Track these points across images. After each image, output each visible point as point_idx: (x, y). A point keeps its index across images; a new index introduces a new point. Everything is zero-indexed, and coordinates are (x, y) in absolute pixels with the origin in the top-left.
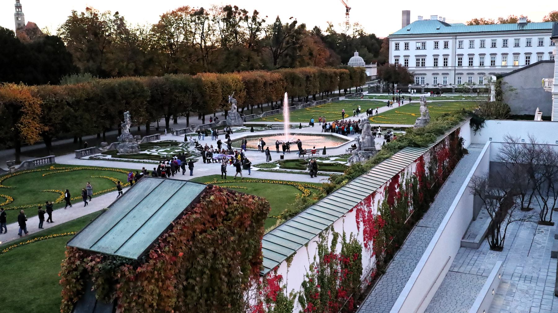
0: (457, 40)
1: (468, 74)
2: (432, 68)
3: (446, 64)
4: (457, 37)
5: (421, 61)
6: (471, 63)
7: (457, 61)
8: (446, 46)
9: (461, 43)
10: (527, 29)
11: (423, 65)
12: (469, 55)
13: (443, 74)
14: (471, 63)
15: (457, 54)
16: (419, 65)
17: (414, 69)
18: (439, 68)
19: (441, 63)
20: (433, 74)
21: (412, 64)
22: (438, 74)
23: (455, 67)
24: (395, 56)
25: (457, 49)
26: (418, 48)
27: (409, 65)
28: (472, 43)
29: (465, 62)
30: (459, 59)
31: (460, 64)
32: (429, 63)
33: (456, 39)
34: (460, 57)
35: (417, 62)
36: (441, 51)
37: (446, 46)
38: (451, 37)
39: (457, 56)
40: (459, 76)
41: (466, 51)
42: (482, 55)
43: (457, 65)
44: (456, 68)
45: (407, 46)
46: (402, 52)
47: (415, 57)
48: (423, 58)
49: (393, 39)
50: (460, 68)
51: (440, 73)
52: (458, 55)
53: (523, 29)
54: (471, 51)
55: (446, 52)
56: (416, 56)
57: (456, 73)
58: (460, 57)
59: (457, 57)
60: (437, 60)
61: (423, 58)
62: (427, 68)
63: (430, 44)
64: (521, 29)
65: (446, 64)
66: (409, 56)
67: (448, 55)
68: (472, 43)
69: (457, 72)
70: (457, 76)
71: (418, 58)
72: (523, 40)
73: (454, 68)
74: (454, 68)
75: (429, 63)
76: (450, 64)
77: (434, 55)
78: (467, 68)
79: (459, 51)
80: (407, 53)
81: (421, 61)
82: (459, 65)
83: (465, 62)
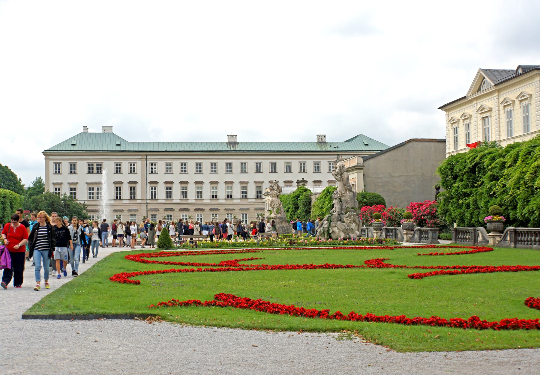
3: (133, 195)
4: (148, 157)
5: (95, 191)
6: (169, 195)
7: (149, 191)
8: (133, 169)
10: (239, 149)
12: (166, 183)
13: (130, 210)
14: (169, 195)
15: (148, 181)
16: (93, 198)
18: (124, 202)
19: (126, 193)
21: (82, 196)
22: (122, 210)
23: (147, 200)
24: (54, 184)
25: (148, 175)
27: (78, 197)
28: (169, 166)
29: (161, 193)
30: (152, 189)
31: (154, 196)
33: (146, 159)
34: (154, 185)
35: (90, 193)
36: (125, 177)
37: (133, 169)
38: (140, 157)
39: (148, 185)
40: (154, 213)
41: (161, 177)
42: (184, 184)
43: (149, 197)
44: (149, 201)
45: (73, 170)
46: (65, 178)
47: (86, 186)
49: (50, 157)
50: (154, 202)
51: (126, 208)
52: (151, 183)
53: (235, 149)
54: (169, 178)
55: (133, 178)
56: (88, 183)
57: (149, 208)
58: (154, 185)
59: (149, 186)
60: (120, 190)
64: (232, 149)
65: (133, 195)
66: (76, 183)
67: (136, 183)
68: (169, 166)
69: (149, 208)
71: (91, 186)
72: (236, 164)
73: (145, 202)
74: (145, 202)
76: (139, 195)
77: (115, 183)
78: (163, 202)
79: (152, 178)
80: (73, 178)
81: (95, 191)
82: (152, 197)
83: (161, 193)
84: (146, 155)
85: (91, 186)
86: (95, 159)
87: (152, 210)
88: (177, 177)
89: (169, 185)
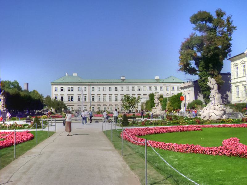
0: (91, 87)
1: (104, 105)
2: (77, 102)
6: (99, 99)
7: (91, 98)
9: (93, 88)
11: (72, 100)
14: (99, 99)
17: (67, 102)
20: (78, 105)
24: (55, 95)
26: (69, 90)
31: (93, 100)
32: (76, 98)
33: (90, 86)
41: (96, 92)
48: (72, 96)
52: (92, 95)
54: (99, 93)
58: (93, 96)
59: (91, 96)
61: (72, 96)
62: (74, 102)
63: (76, 88)
67: (86, 95)
69: (91, 104)
70: (91, 106)
75: (76, 98)
76: (87, 99)
79: (92, 93)
84: (90, 84)
85: (69, 96)
86: (70, 86)
87: (92, 105)
88: (102, 92)
89: (99, 96)
